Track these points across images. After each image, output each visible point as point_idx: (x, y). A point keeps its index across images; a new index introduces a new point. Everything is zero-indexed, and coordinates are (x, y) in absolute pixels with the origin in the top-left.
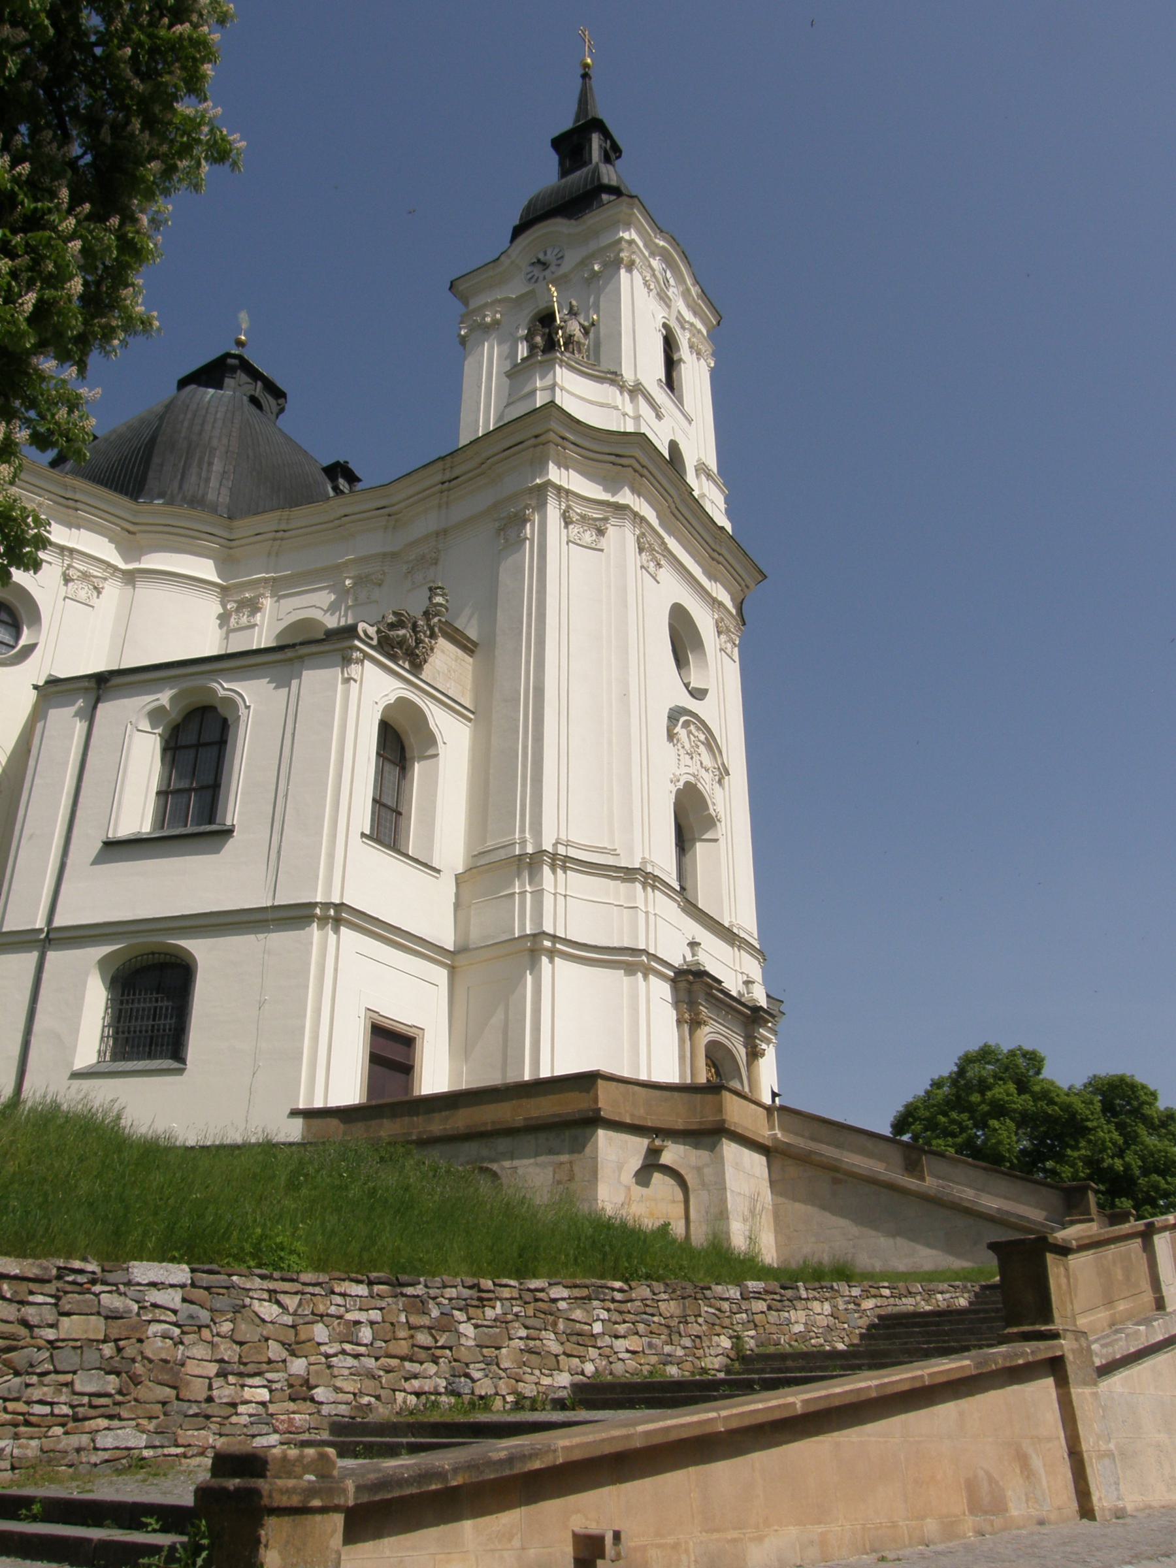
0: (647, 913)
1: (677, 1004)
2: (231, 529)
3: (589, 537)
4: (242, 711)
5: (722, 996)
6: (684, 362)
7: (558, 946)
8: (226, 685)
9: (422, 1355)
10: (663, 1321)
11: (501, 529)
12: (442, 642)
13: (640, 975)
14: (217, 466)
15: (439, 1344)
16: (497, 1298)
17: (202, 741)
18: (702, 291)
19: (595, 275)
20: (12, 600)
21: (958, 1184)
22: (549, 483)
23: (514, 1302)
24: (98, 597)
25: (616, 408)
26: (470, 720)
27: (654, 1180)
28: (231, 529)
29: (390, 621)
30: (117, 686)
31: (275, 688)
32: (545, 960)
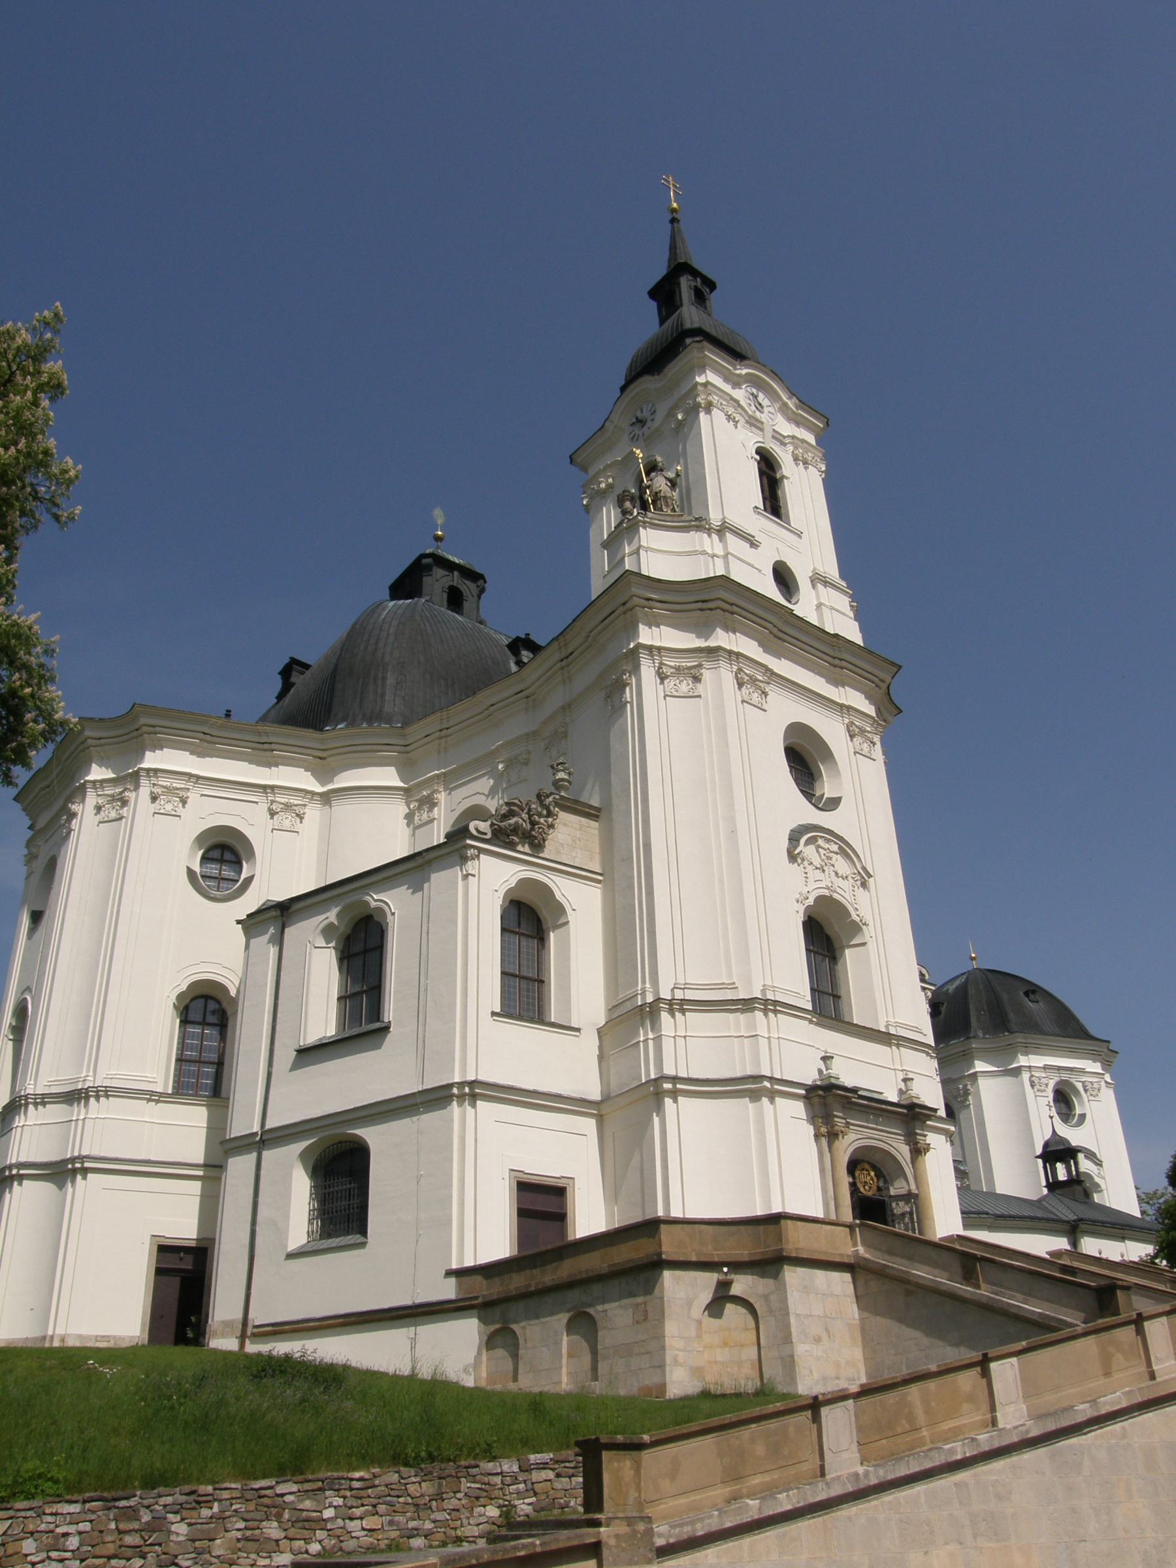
0: (769, 1038)
1: (812, 1119)
2: (404, 736)
3: (685, 687)
4: (389, 918)
5: (866, 1102)
6: (787, 478)
7: (679, 1086)
8: (375, 897)
9: (129, 1552)
10: (410, 1500)
11: (608, 696)
12: (563, 816)
13: (765, 1100)
14: (391, 680)
15: (148, 1543)
16: (215, 1500)
17: (367, 948)
18: (800, 401)
19: (680, 424)
20: (227, 840)
21: (1010, 1289)
22: (639, 646)
23: (234, 1501)
24: (301, 822)
25: (704, 553)
26: (599, 882)
27: (726, 1311)
28: (404, 736)
29: (502, 812)
30: (295, 911)
31: (413, 893)
32: (668, 1101)
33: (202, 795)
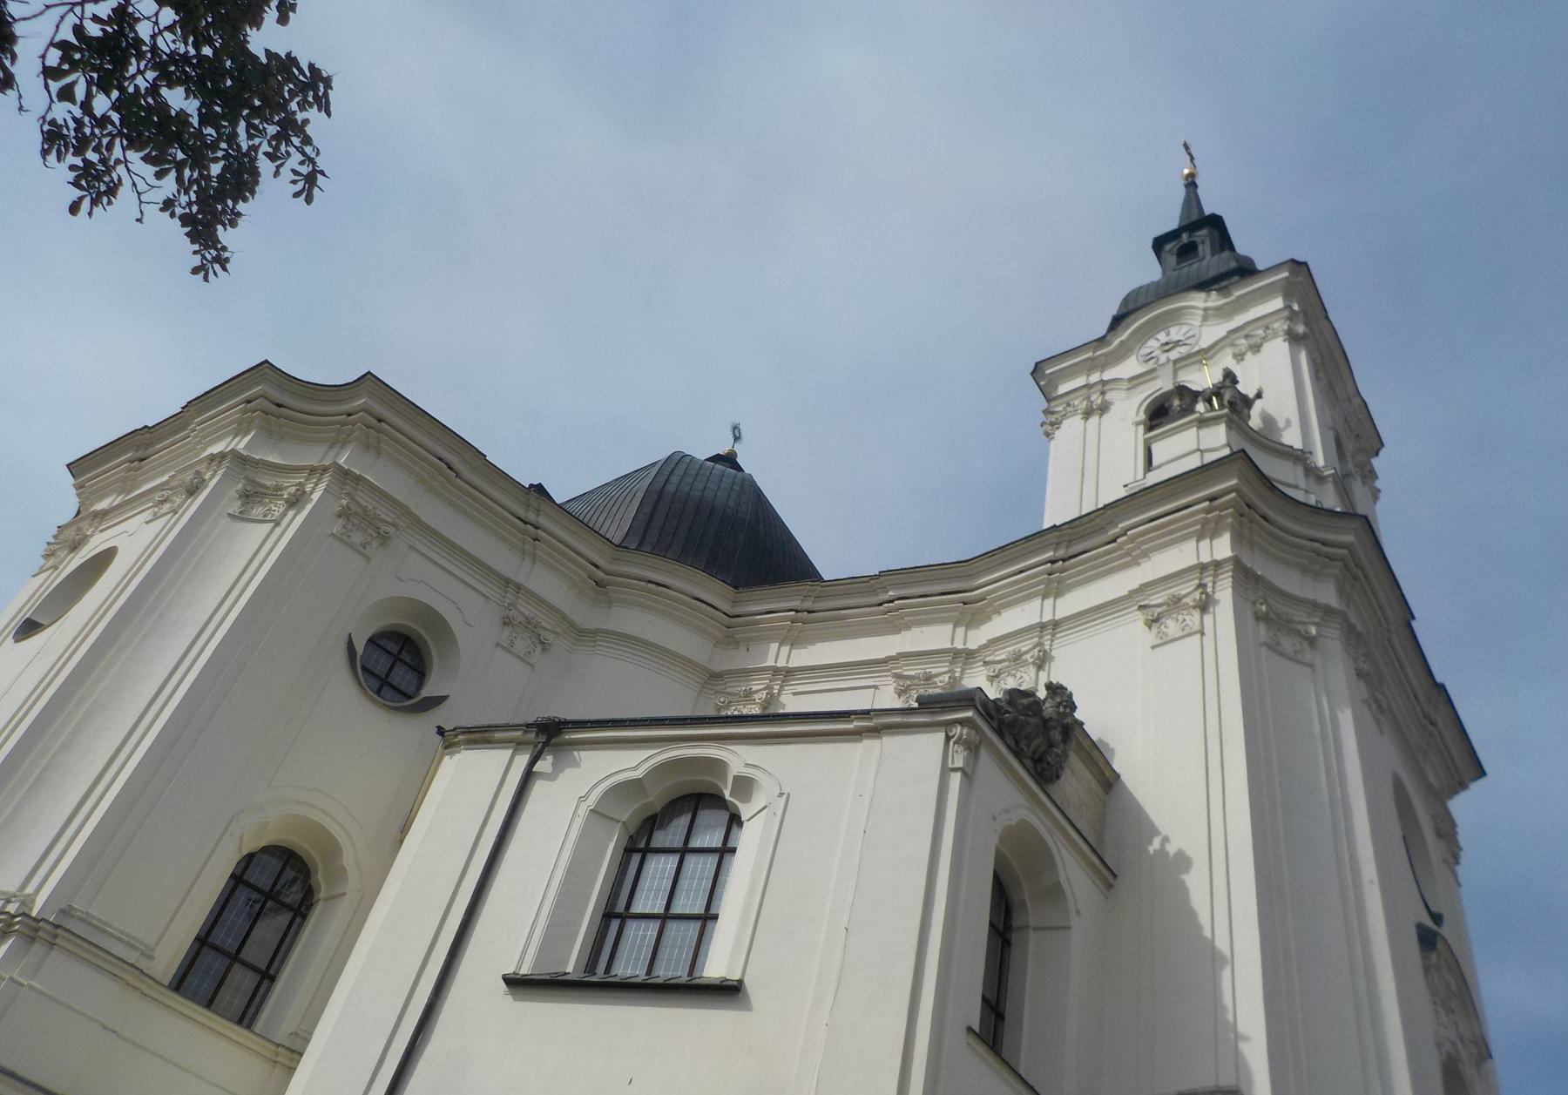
20: (423, 633)
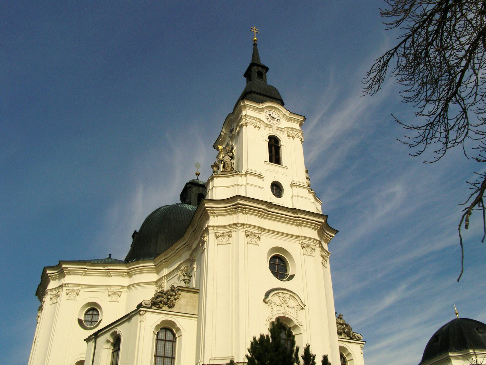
26: (196, 318)
33: (84, 291)
